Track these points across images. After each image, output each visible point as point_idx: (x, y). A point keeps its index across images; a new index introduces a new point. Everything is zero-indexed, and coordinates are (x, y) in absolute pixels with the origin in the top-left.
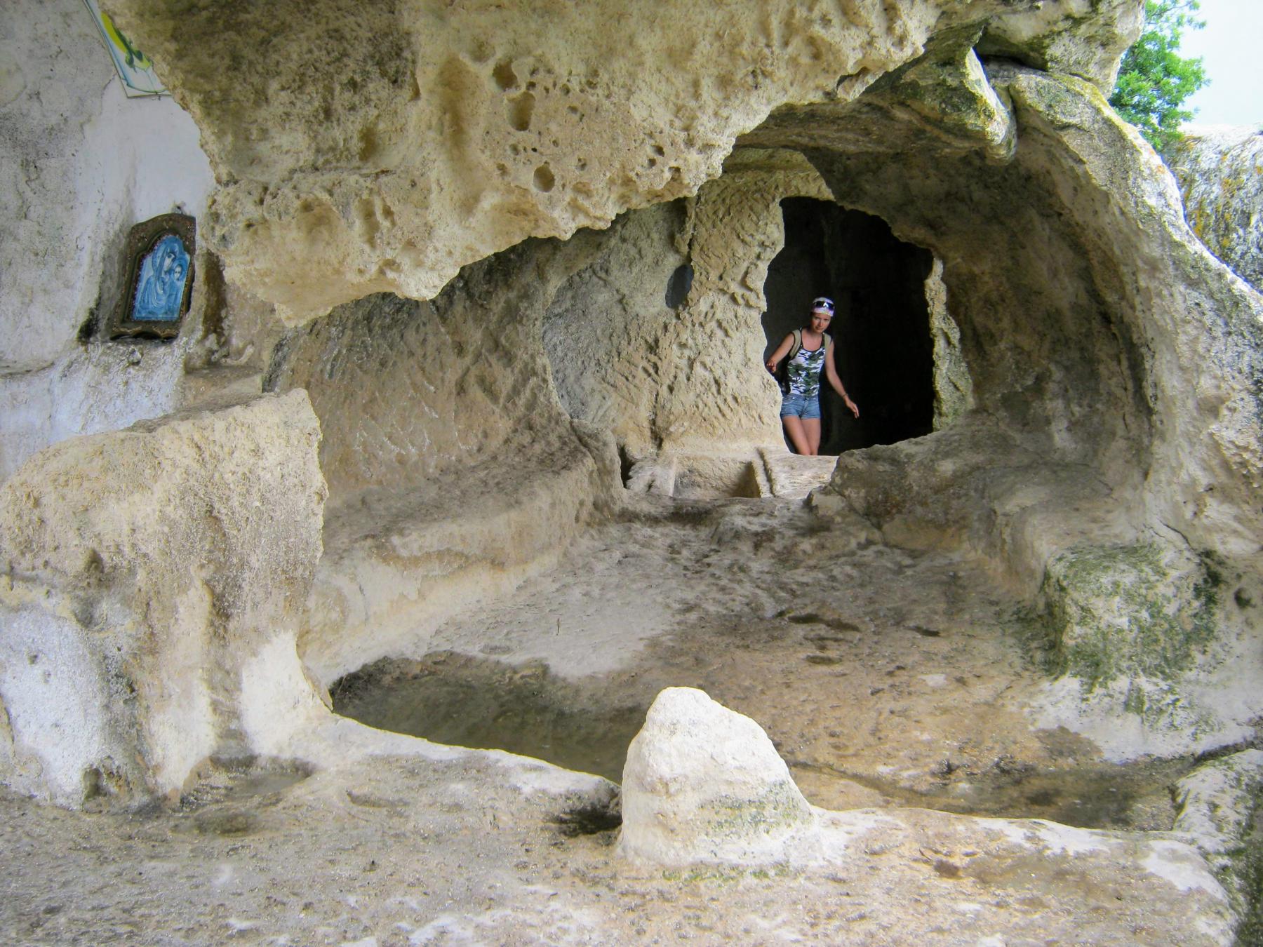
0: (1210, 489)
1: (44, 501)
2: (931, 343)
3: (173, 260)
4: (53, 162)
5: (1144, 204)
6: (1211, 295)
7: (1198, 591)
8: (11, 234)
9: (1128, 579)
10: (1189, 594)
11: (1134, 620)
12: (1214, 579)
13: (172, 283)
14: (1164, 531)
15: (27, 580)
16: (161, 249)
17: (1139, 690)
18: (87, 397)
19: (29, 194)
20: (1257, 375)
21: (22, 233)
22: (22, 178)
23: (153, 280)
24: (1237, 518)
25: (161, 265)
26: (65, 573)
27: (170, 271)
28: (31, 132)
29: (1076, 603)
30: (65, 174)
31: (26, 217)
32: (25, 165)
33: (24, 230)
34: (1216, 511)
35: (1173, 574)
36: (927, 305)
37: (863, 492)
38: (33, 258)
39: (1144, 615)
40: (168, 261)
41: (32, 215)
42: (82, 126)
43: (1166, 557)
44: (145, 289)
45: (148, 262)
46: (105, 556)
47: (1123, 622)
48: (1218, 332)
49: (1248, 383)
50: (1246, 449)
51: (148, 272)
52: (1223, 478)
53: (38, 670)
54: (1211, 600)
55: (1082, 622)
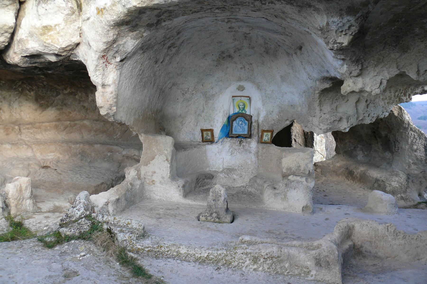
0: (413, 163)
1: (299, 163)
2: (291, 142)
3: (242, 122)
4: (211, 101)
5: (406, 119)
6: (417, 133)
7: (406, 181)
8: (200, 115)
9: (397, 179)
10: (405, 181)
11: (399, 185)
12: (408, 178)
13: (243, 127)
14: (399, 171)
15: (296, 176)
16: (238, 120)
17: (402, 196)
18: (230, 149)
19: (205, 107)
20: (425, 145)
21: (202, 115)
22: (205, 104)
23: (237, 126)
24: (417, 168)
25: (239, 123)
26: (305, 174)
27: (242, 124)
28: (209, 95)
29: (388, 184)
30: (213, 104)
31: (203, 112)
32: (206, 101)
33: (203, 114)
34: (413, 167)
35: (403, 178)
36: (291, 133)
37: (320, 170)
38: (204, 120)
39: (400, 185)
40: (240, 123)
41: (205, 111)
42: (219, 94)
43: (401, 175)
44: (235, 128)
45: (234, 122)
46: (311, 171)
47: (397, 186)
48: (418, 139)
49: (423, 146)
50: (422, 156)
51: (235, 124)
52: (416, 161)
53: (296, 191)
54: (408, 182)
55: (389, 187)
